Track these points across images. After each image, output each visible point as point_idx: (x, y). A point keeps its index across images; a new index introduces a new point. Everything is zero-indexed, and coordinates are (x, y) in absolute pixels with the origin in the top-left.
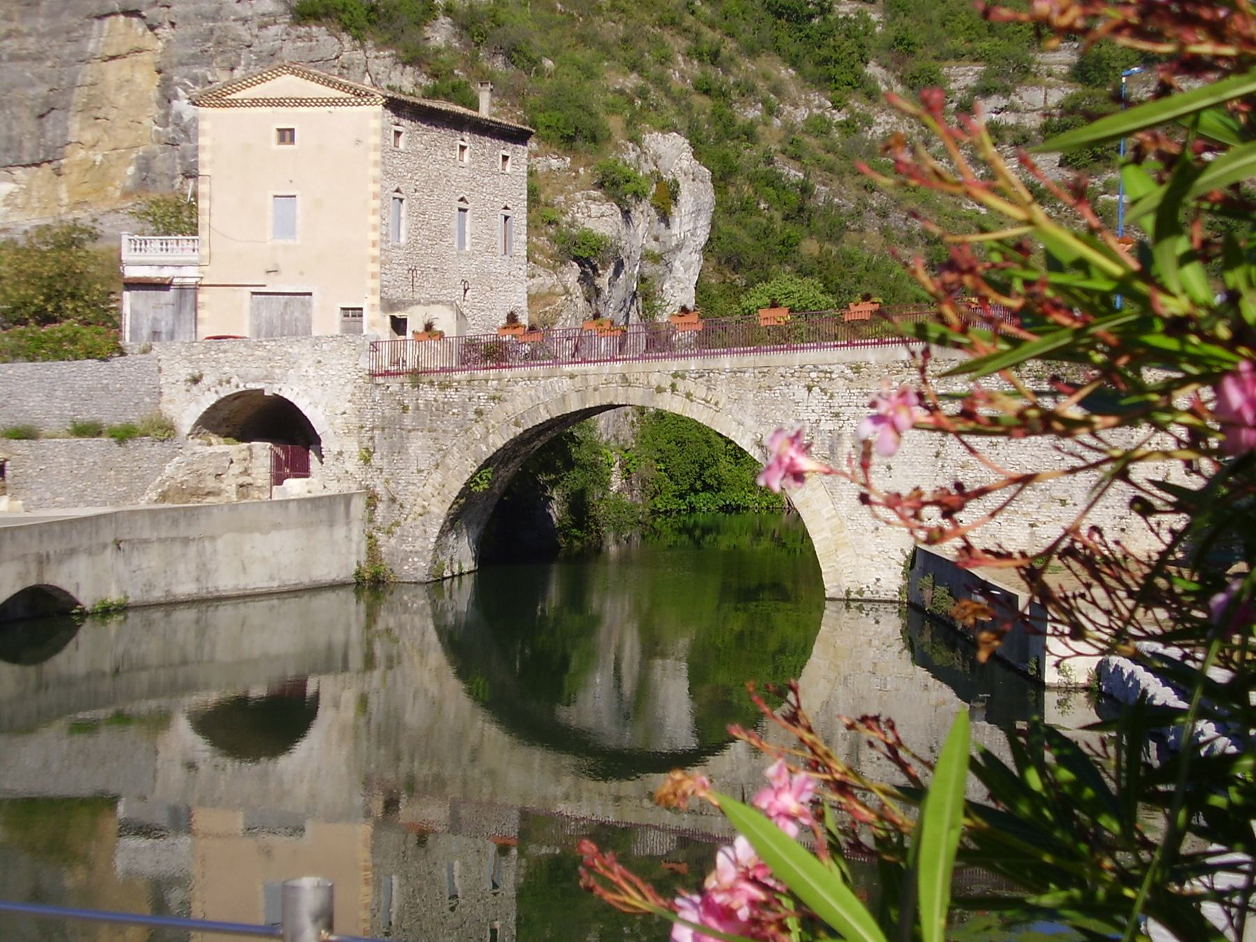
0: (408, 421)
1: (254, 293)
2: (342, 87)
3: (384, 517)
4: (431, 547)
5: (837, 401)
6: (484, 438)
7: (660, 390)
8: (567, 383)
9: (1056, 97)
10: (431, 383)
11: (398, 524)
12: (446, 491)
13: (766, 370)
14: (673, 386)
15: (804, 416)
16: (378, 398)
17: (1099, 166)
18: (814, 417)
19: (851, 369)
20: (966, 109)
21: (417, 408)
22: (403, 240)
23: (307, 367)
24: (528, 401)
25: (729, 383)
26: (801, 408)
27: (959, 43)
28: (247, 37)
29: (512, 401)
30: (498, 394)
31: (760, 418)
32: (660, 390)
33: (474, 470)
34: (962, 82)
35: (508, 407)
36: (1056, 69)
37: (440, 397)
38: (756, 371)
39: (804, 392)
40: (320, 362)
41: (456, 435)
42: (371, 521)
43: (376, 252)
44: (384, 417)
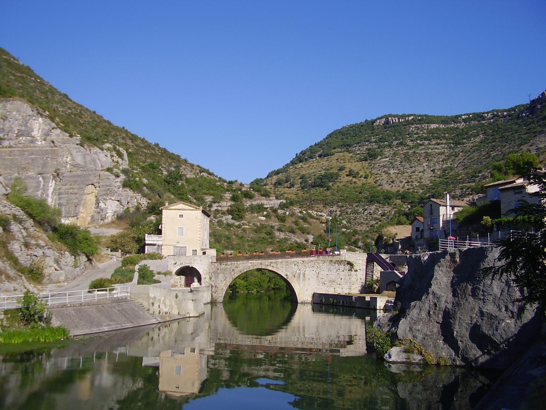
2: (193, 207)
5: (300, 267)
6: (234, 275)
7: (268, 265)
8: (250, 264)
9: (229, 204)
17: (240, 219)
20: (210, 206)
23: (199, 261)
27: (205, 191)
28: (116, 190)
31: (286, 271)
32: (268, 265)
34: (208, 200)
35: (239, 269)
36: (228, 198)
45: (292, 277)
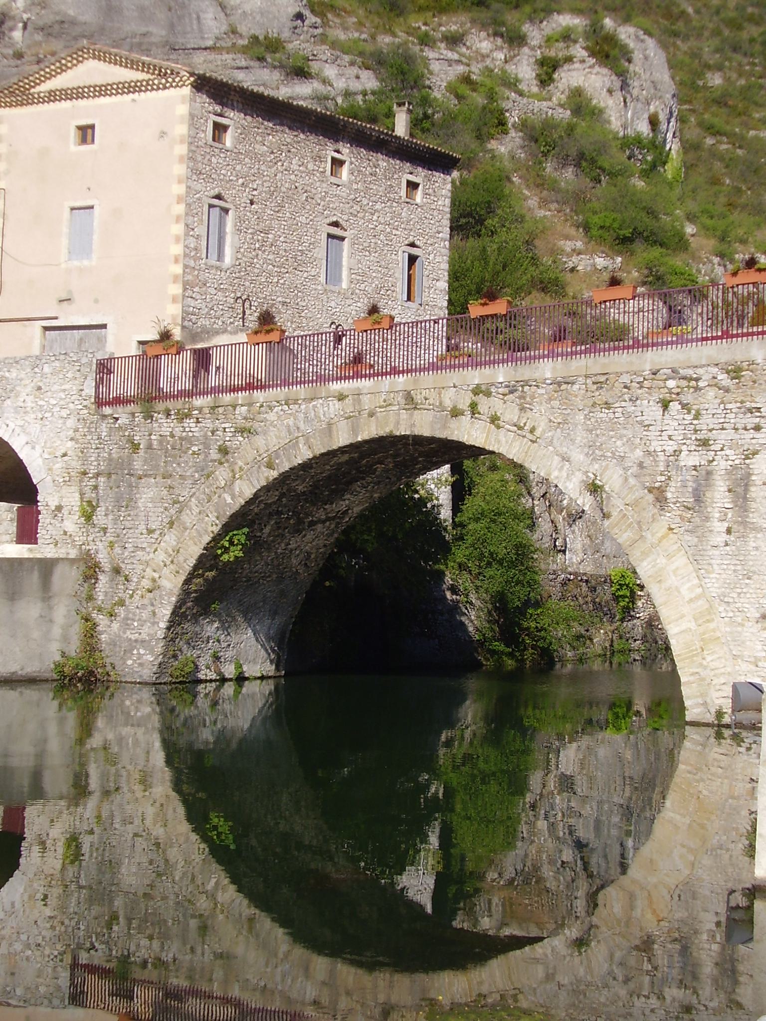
0: (138, 465)
1: (46, 329)
3: (106, 593)
4: (161, 634)
5: (706, 421)
6: (229, 485)
7: (456, 413)
8: (334, 407)
10: (168, 414)
11: (122, 603)
12: (181, 559)
13: (602, 379)
14: (473, 406)
15: (655, 446)
16: (104, 434)
18: (671, 447)
19: (728, 372)
21: (150, 447)
22: (228, 260)
24: (284, 434)
25: (550, 399)
26: (653, 433)
29: (265, 433)
30: (248, 425)
31: (593, 450)
33: (216, 529)
35: (259, 441)
37: (178, 431)
38: (589, 381)
39: (658, 410)
40: (39, 388)
41: (195, 483)
42: (90, 598)
43: (178, 269)
44: (110, 460)
45: (635, 504)
